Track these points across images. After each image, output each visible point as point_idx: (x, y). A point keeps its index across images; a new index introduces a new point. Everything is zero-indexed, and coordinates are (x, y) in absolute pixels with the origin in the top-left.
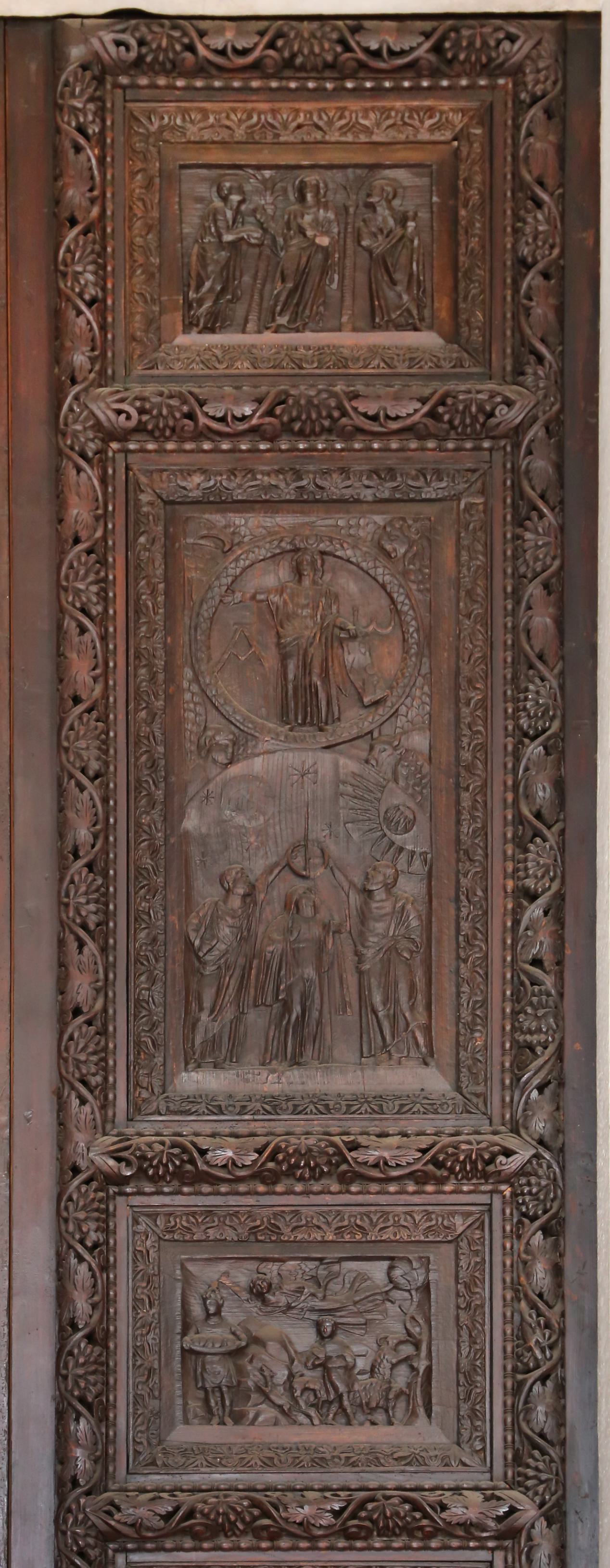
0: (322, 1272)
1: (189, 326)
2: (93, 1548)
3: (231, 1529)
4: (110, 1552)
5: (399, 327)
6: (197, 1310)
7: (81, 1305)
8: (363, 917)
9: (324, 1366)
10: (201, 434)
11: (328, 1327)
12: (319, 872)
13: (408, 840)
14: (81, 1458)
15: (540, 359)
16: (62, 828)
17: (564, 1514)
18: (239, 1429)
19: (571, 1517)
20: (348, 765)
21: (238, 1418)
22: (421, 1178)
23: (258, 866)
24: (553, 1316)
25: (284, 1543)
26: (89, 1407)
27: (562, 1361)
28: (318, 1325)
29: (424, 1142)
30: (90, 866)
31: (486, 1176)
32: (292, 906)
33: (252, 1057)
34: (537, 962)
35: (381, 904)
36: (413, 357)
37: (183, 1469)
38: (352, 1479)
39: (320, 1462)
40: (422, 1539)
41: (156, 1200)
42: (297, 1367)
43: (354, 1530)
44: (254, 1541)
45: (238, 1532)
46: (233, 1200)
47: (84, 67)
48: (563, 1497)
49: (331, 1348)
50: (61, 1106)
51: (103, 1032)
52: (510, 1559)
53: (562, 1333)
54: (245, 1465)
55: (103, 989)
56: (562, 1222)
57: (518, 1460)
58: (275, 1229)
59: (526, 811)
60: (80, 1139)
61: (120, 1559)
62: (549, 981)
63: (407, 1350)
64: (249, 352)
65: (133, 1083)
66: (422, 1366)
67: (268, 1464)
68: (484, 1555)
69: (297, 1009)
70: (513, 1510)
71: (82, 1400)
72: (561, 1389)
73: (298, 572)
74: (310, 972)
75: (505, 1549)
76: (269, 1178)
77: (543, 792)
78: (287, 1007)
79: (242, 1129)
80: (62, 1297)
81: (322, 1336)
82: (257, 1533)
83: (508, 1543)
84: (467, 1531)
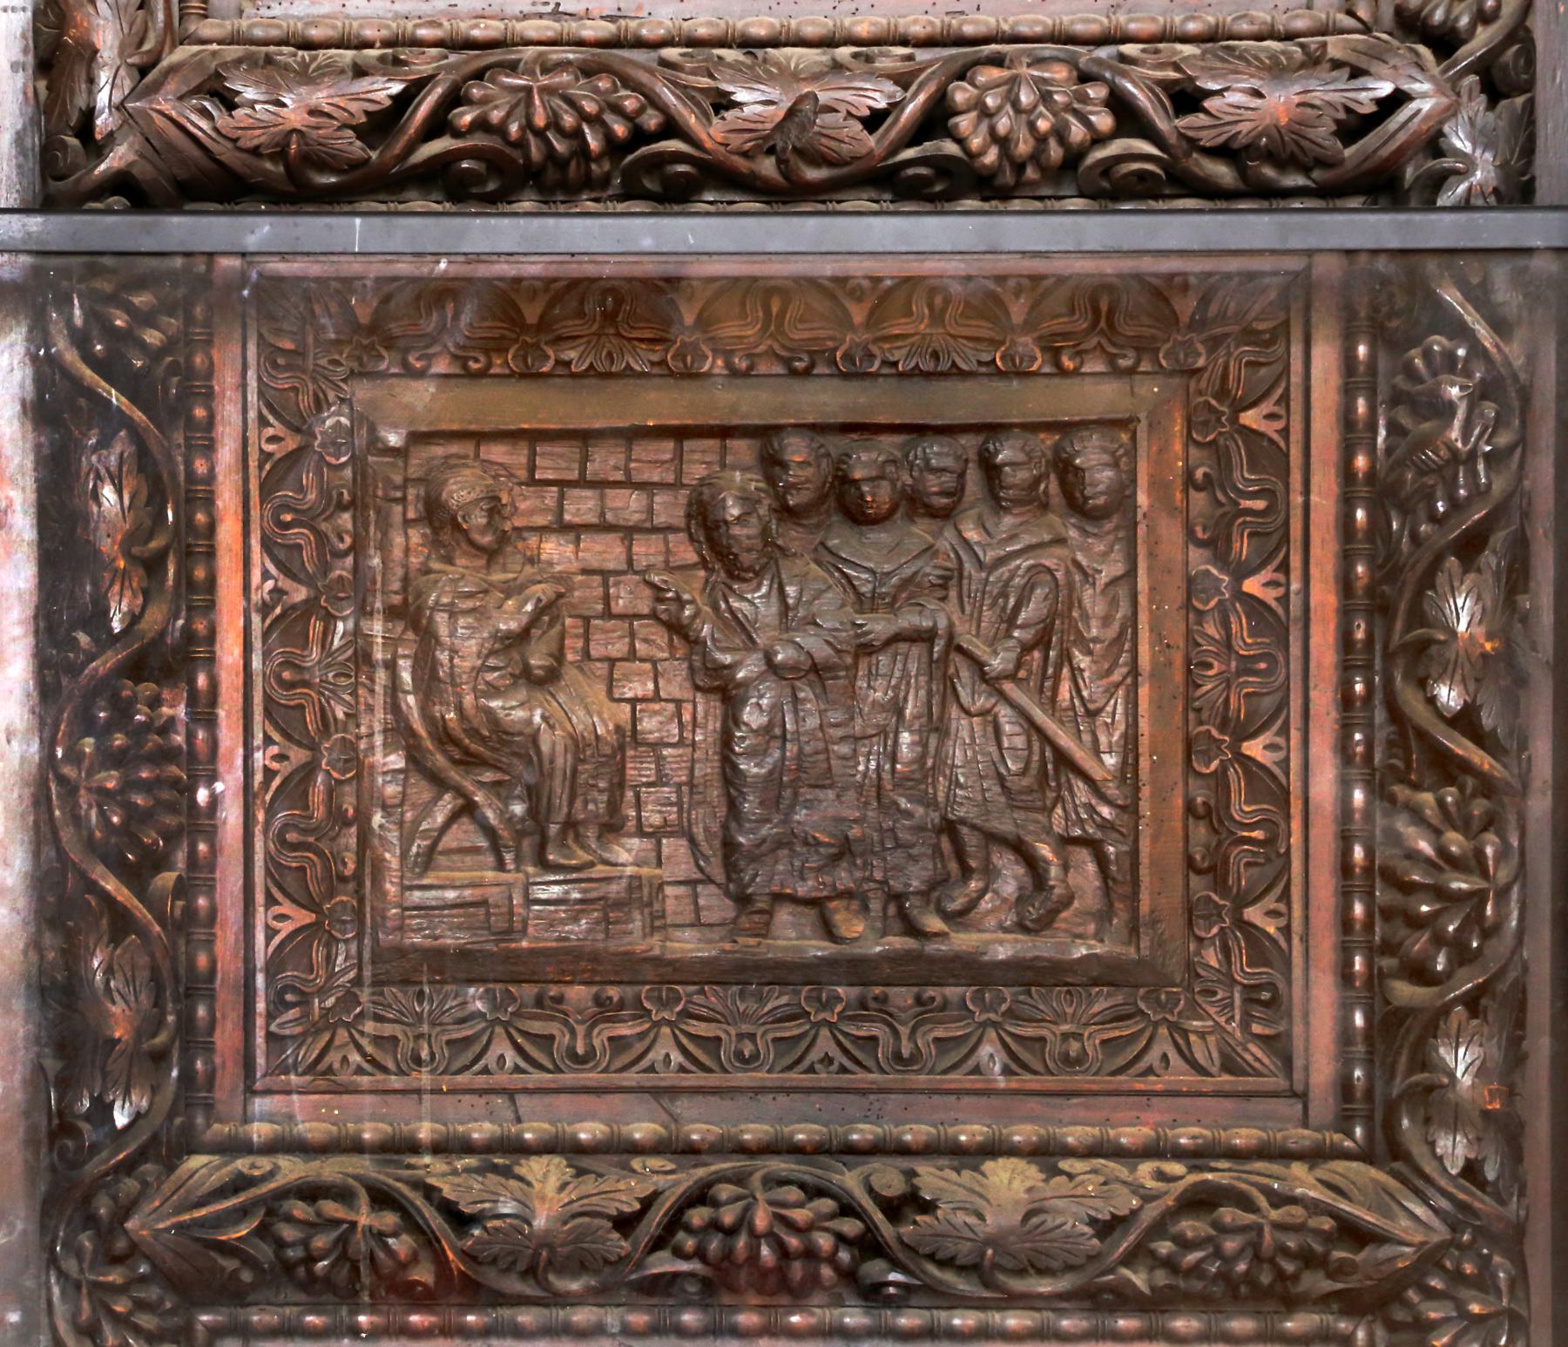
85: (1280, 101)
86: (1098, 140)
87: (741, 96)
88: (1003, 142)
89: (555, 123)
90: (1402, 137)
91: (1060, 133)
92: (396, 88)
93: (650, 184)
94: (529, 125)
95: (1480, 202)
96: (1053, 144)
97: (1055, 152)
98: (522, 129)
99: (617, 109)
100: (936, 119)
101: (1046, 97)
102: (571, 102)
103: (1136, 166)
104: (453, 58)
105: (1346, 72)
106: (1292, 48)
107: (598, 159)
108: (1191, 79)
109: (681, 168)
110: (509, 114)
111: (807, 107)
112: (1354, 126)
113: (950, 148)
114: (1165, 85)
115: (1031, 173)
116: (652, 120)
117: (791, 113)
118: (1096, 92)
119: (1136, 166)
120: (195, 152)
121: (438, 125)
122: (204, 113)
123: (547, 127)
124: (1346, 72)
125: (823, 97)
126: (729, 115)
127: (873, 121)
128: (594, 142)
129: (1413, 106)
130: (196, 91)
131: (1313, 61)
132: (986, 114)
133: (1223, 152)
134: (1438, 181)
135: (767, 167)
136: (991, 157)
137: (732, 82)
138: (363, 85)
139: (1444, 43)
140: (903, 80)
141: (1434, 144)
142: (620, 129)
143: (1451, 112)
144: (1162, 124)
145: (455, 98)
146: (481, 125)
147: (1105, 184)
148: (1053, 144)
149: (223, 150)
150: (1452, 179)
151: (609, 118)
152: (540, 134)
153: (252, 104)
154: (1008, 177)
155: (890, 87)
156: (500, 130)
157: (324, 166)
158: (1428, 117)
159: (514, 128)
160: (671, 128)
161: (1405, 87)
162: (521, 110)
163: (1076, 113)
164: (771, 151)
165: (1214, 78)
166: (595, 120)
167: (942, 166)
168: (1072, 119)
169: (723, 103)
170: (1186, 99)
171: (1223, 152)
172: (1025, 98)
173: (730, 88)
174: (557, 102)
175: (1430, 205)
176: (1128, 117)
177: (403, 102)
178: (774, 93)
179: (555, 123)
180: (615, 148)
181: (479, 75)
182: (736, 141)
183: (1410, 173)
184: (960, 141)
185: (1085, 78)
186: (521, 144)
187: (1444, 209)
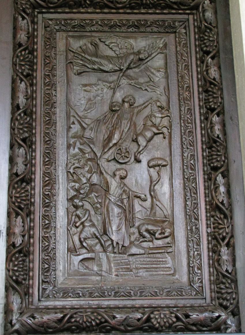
2: (29, 9)
3: (85, 4)
4: (36, 13)
25: (106, 10)
40: (160, 10)
43: (133, 4)
44: (94, 10)
45: (87, 5)
52: (195, 18)
61: (40, 16)
68: (186, 16)
75: (193, 14)
83: (194, 12)
84: (178, 6)
85: (202, 316)
86: (174, 323)
87: (117, 316)
88: (159, 323)
89: (87, 321)
90: (221, 322)
91: (168, 322)
92: (62, 315)
93: (104, 330)
94: (83, 321)
95: (233, 332)
96: (167, 323)
97: (167, 324)
98: (82, 322)
99: (97, 319)
100: (148, 319)
101: (165, 316)
102: (90, 318)
103: (180, 327)
104: (72, 310)
105: (211, 312)
106: (203, 308)
107: (95, 326)
108: (188, 313)
109: (109, 328)
110: (80, 319)
111: (128, 318)
113: (151, 324)
114: (184, 314)
115: (164, 328)
116: (103, 320)
117: (125, 319)
118: (173, 315)
119: (180, 327)
120: (29, 326)
121: (69, 321)
122: (30, 320)
123: (86, 321)
124: (211, 312)
125: (130, 316)
126: (116, 319)
127: (139, 320)
128: (94, 323)
129: (222, 317)
130: (30, 316)
132: (156, 319)
133: (194, 325)
134: (226, 329)
135: (122, 328)
136: (157, 325)
137: (116, 314)
138: (56, 315)
139: (226, 308)
140: (143, 314)
141: (225, 323)
142: (98, 321)
143: (228, 318)
144: (184, 320)
145: (71, 317)
146: (75, 321)
147: (176, 330)
148: (167, 323)
149: (34, 326)
150: (229, 328)
151: (96, 320)
152: (85, 322)
153: (38, 318)
154: (160, 329)
155: (141, 314)
156: (79, 322)
157: (50, 328)
158: (224, 319)
159: (81, 322)
160: (106, 321)
161: (220, 314)
162: (82, 319)
163: (170, 318)
164: (123, 325)
165: (191, 313)
166: (94, 320)
167: (150, 327)
168: (169, 319)
169: (114, 317)
170: (187, 316)
171: (194, 325)
172: (162, 316)
173: (116, 315)
174: (88, 318)
175: (226, 333)
177: (63, 317)
178: (122, 316)
179: (87, 321)
180: (97, 325)
181: (76, 313)
182: (117, 323)
183: (222, 327)
184: (152, 323)
185: (171, 313)
186: (82, 324)
187: (228, 333)
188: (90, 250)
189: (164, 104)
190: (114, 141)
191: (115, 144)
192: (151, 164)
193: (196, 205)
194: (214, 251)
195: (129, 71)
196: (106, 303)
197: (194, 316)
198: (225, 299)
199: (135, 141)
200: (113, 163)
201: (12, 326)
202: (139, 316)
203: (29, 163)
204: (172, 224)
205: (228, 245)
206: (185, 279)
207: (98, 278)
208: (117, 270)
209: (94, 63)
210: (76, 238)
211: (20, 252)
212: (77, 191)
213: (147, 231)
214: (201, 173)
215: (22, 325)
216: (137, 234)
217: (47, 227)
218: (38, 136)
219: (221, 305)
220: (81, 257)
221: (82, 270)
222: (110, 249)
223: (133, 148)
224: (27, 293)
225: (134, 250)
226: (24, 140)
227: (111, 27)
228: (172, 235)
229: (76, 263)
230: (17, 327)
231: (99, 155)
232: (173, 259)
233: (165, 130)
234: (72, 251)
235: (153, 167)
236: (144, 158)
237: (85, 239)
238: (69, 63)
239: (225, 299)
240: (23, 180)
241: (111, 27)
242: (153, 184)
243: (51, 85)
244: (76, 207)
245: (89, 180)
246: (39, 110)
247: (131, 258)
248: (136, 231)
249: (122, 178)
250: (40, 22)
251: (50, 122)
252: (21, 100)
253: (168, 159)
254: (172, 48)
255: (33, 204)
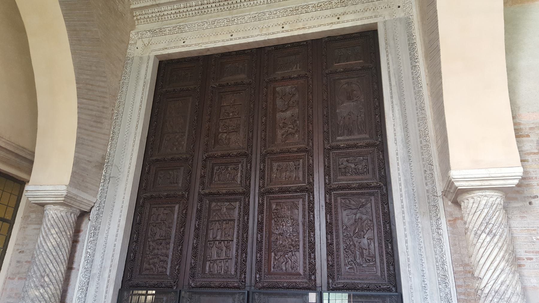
0: (355, 158)
1: (336, 63)
5: (358, 60)
6: (340, 163)
7: (326, 163)
8: (357, 119)
9: (355, 169)
10: (337, 73)
11: (356, 164)
12: (352, 115)
13: (362, 110)
14: (327, 181)
15: (373, 61)
16: (323, 113)
17: (387, 185)
18: (346, 177)
19: (388, 185)
20: (355, 103)
21: (346, 176)
22: (366, 147)
23: (345, 115)
24: (383, 161)
25: (352, 190)
26: (328, 175)
27: (385, 167)
28: (355, 164)
29: (366, 143)
30: (326, 116)
31: (374, 146)
32: (349, 118)
33: (345, 135)
34: (378, 122)
35: (359, 117)
36: (360, 63)
37: (339, 181)
38: (360, 182)
39: (356, 180)
41: (335, 151)
42: (352, 169)
46: (344, 151)
47: (324, 42)
48: (386, 183)
49: (356, 167)
50: (324, 142)
51: (328, 133)
53: (385, 163)
54: (346, 181)
55: (328, 129)
56: (384, 151)
57: (380, 179)
58: (349, 154)
59: (375, 106)
60: (326, 145)
61: (332, 192)
62: (379, 124)
63: (366, 166)
64: (341, 65)
65: (332, 139)
66: (368, 168)
67: (349, 181)
68: (377, 190)
69: (350, 129)
70: (380, 185)
71: (327, 174)
72: (385, 170)
73: (348, 85)
74: (352, 125)
76: (348, 148)
77: (377, 104)
78: (349, 130)
79: (344, 143)
80: (324, 163)
81: (355, 166)
82: (349, 189)
100: (369, 287)
112: (388, 288)
131: (386, 285)
139: (392, 284)
145: (346, 286)
170: (380, 287)
176: (377, 287)
188: (351, 265)
189: (371, 219)
190: (357, 231)
191: (357, 232)
192: (369, 238)
193: (382, 252)
194: (388, 267)
195: (360, 209)
196: (356, 282)
197: (382, 287)
198: (391, 282)
199: (363, 231)
200: (356, 238)
201: (330, 288)
202: (366, 286)
203: (332, 239)
204: (375, 257)
205: (392, 265)
206: (380, 275)
207: (354, 274)
208: (359, 271)
209: (349, 206)
210: (347, 261)
211: (331, 266)
212: (346, 247)
213: (368, 259)
214: (384, 242)
215: (332, 287)
216: (364, 261)
217: (338, 258)
218: (334, 230)
219: (390, 284)
220: (348, 267)
221: (349, 271)
222: (357, 265)
223: (362, 233)
224: (333, 278)
225: (364, 265)
226: (330, 232)
227: (354, 195)
228: (375, 261)
229: (347, 269)
230: (331, 288)
231: (352, 236)
232: (376, 269)
233: (372, 228)
234: (346, 265)
235: (369, 239)
236: (366, 236)
237: (349, 262)
238: (342, 207)
239: (391, 282)
240: (330, 244)
241: (354, 195)
242: (369, 245)
243: (336, 214)
244: (346, 252)
245: (349, 243)
246: (334, 222)
247: (363, 268)
248: (364, 259)
249: (359, 243)
250: (332, 194)
251: (337, 226)
252: (329, 221)
253: (373, 237)
254: (373, 202)
255: (333, 251)
